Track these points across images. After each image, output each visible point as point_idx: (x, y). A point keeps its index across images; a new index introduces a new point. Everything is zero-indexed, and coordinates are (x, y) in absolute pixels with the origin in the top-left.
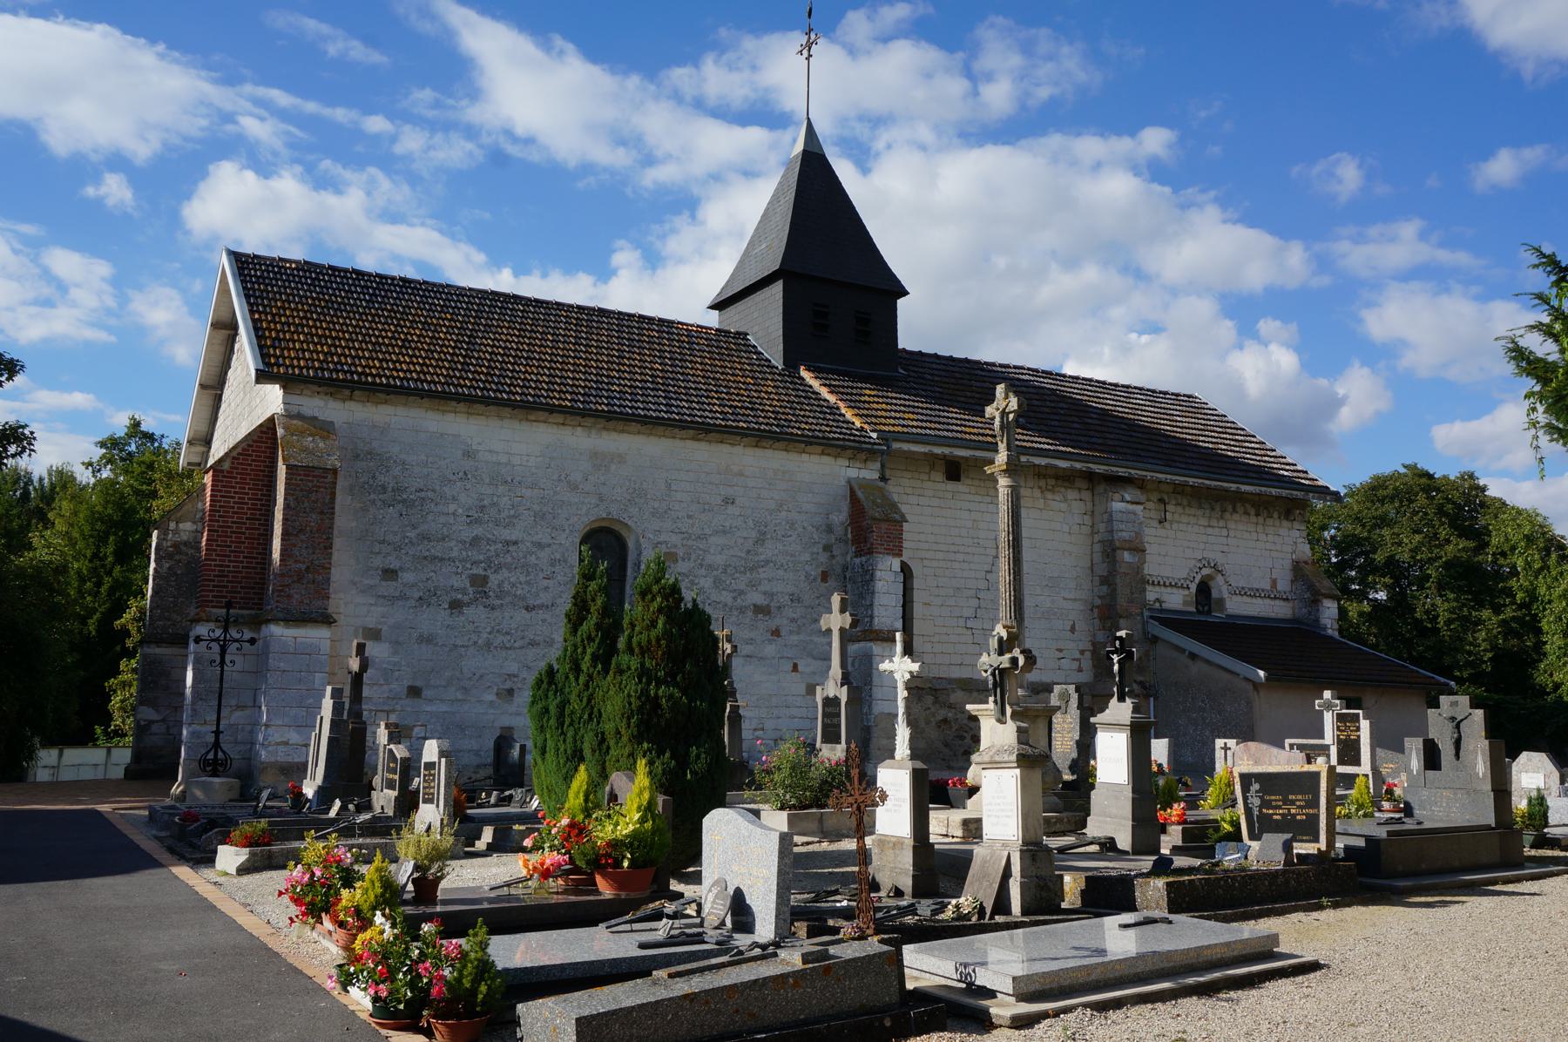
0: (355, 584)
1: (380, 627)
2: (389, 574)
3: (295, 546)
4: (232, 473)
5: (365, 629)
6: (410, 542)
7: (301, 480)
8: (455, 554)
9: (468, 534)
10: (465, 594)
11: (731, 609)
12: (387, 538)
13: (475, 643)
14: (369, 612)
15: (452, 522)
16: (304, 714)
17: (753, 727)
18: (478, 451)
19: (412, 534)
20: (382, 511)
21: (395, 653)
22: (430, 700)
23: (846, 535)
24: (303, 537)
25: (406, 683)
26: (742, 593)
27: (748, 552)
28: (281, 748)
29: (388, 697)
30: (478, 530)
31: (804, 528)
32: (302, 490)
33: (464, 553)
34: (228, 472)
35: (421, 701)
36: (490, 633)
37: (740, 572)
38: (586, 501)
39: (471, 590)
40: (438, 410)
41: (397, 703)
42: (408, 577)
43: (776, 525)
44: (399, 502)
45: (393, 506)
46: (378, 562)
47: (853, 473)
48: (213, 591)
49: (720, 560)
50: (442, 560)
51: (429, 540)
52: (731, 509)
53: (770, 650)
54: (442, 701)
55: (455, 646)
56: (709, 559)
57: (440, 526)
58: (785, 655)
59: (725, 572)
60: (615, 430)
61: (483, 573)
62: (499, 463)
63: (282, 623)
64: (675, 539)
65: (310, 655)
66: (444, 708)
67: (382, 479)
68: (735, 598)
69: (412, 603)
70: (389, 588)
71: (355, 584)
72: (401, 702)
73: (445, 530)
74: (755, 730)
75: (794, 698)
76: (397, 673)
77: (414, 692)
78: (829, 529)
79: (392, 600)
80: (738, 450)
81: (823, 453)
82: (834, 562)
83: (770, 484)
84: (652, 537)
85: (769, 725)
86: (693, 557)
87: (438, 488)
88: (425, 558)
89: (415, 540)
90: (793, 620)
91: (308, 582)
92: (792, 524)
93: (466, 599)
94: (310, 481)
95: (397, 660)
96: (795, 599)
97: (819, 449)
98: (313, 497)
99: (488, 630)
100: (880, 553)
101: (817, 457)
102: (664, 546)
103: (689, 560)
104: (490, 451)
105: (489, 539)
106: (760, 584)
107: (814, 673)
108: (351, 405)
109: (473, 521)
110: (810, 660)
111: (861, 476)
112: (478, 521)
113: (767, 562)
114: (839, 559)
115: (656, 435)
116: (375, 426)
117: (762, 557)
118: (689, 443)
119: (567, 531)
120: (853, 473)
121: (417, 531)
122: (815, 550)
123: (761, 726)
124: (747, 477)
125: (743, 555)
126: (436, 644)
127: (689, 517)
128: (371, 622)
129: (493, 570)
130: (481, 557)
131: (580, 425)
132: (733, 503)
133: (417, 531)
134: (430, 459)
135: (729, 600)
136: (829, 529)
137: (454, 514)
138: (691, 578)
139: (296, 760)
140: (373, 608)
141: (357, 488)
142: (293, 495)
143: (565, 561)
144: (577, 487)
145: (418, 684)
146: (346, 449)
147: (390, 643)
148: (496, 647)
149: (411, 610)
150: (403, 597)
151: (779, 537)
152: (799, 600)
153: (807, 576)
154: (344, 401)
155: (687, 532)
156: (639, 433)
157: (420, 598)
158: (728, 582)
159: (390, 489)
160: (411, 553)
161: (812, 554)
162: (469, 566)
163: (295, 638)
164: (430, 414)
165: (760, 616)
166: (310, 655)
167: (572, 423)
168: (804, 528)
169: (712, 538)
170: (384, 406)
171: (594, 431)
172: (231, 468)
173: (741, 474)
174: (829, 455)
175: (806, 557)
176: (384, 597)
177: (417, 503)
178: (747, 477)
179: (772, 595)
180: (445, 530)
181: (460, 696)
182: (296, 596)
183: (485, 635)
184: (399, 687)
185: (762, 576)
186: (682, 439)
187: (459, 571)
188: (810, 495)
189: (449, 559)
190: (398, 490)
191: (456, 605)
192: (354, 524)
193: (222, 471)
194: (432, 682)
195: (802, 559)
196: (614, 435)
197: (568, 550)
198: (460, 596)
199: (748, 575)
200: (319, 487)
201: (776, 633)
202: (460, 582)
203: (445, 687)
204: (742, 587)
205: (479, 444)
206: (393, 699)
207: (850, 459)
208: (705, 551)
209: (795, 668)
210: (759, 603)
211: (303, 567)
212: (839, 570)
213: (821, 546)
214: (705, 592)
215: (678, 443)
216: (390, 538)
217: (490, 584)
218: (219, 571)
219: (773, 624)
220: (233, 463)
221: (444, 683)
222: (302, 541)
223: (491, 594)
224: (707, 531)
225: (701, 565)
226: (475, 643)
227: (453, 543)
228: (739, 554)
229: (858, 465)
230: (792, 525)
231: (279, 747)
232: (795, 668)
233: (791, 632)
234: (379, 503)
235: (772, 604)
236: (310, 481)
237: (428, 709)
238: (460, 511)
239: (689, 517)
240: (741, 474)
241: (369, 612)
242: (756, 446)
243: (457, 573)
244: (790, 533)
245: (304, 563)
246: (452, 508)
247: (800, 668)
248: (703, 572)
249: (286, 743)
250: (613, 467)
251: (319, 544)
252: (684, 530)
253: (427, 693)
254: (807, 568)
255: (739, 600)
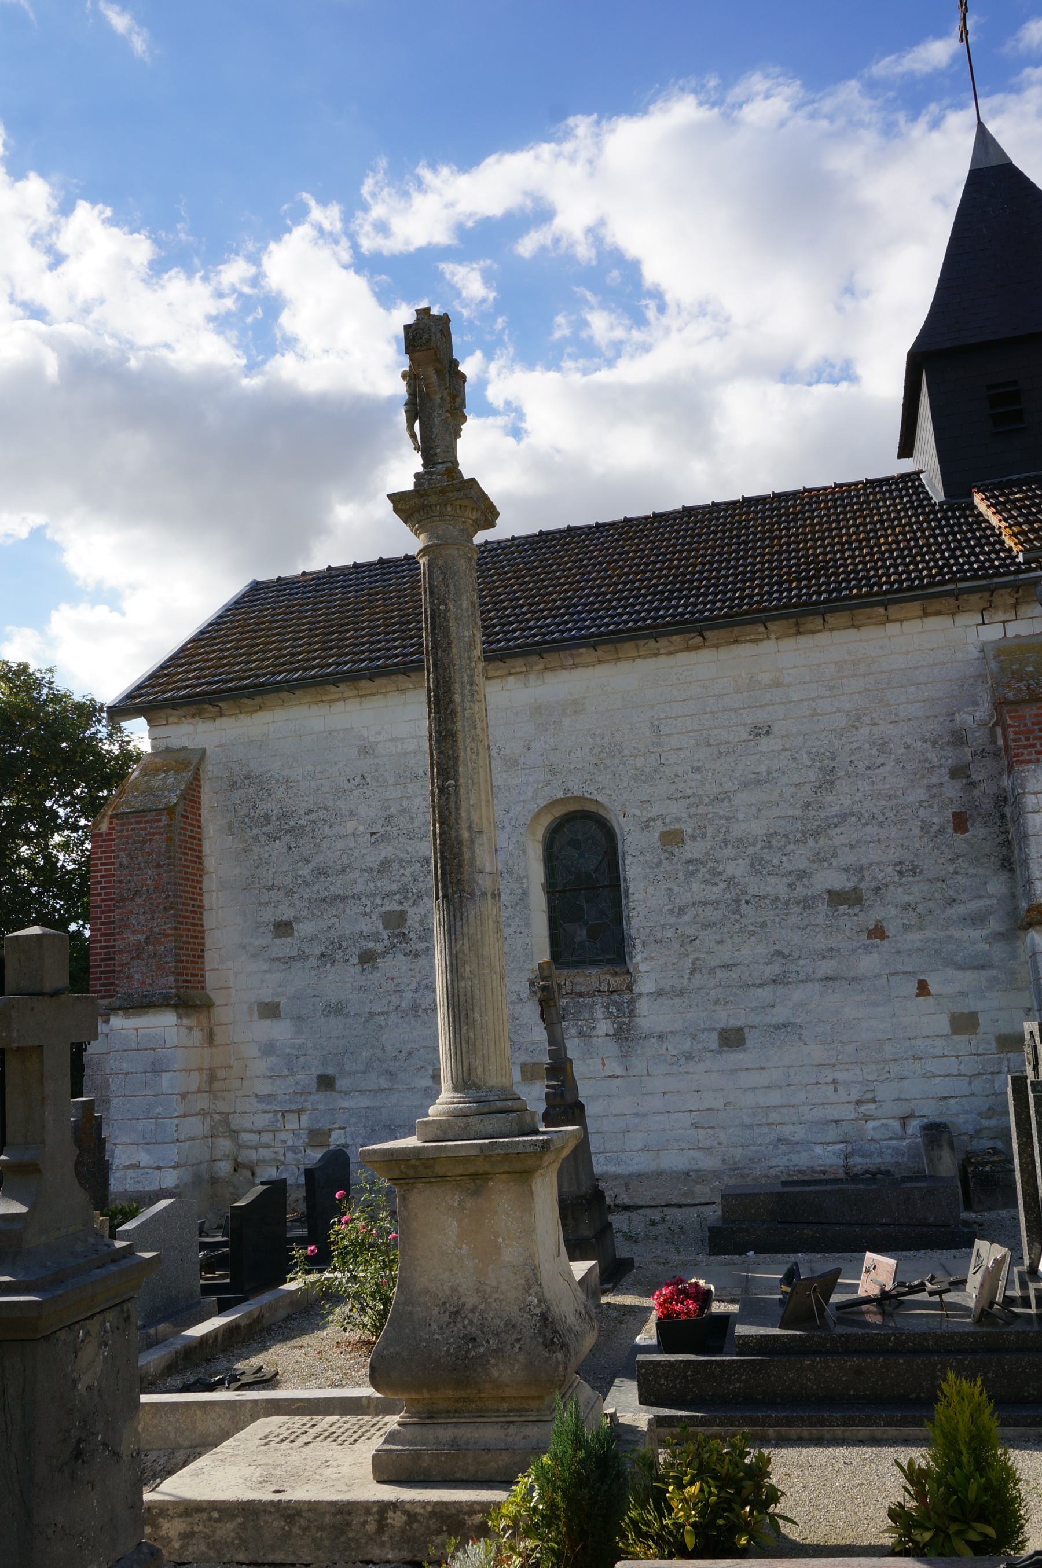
0: (244, 947)
1: (277, 1000)
2: (283, 928)
3: (131, 912)
4: (111, 834)
5: (260, 1004)
6: (304, 881)
7: (132, 830)
8: (359, 888)
9: (373, 859)
10: (378, 941)
11: (787, 904)
12: (276, 882)
13: (398, 1007)
14: (263, 981)
15: (352, 845)
16: (154, 1127)
17: (854, 1098)
18: (377, 743)
19: (305, 871)
20: (267, 848)
21: (299, 1032)
22: (346, 1093)
23: (994, 742)
24: (139, 900)
25: (315, 1072)
26: (802, 875)
27: (807, 805)
28: (130, 1173)
29: (295, 1093)
30: (387, 851)
31: (907, 747)
32: (135, 842)
33: (372, 885)
34: (107, 835)
35: (334, 1094)
36: (416, 991)
37: (797, 842)
38: (531, 779)
39: (385, 934)
40: (323, 701)
41: (306, 1101)
42: (305, 929)
43: (852, 752)
44: (287, 832)
45: (280, 838)
46: (269, 915)
47: (992, 633)
48: (100, 979)
49: (757, 828)
50: (344, 899)
51: (326, 875)
52: (765, 744)
53: (869, 963)
54: (361, 1092)
55: (372, 1014)
56: (738, 830)
57: (339, 853)
58: (900, 968)
59: (769, 845)
60: (563, 667)
61: (399, 908)
62: (406, 754)
63: (121, 1013)
64: (675, 809)
65: (154, 1049)
66: (364, 1102)
67: (264, 806)
68: (791, 886)
69: (314, 962)
70: (285, 946)
71: (244, 947)
72: (311, 1098)
73: (345, 857)
74: (859, 1103)
75: (929, 1042)
76: (302, 1059)
77: (326, 1082)
78: (959, 738)
79: (287, 961)
80: (768, 646)
81: (926, 614)
82: (976, 793)
83: (831, 688)
84: (637, 812)
85: (885, 1092)
86: (710, 830)
87: (330, 804)
88: (324, 900)
89: (309, 878)
90: (907, 907)
91: (149, 956)
92: (883, 744)
93: (380, 947)
94: (142, 829)
95: (300, 1041)
96: (907, 870)
97: (915, 607)
98: (147, 848)
99: (413, 987)
100: (1029, 762)
101: (918, 621)
102: (659, 823)
103: (704, 836)
104: (392, 740)
105: (402, 860)
106: (835, 855)
107: (962, 994)
108: (224, 722)
109: (378, 838)
110: (950, 972)
111: (1010, 634)
112: (385, 838)
113: (844, 817)
114: (988, 788)
115: (627, 659)
116: (252, 741)
117: (835, 810)
118: (683, 657)
119: (508, 829)
120: (992, 633)
121: (311, 866)
122: (934, 780)
123: (869, 1096)
124: (789, 685)
125: (798, 813)
126: (347, 1016)
127: (696, 770)
128: (267, 995)
129: (411, 902)
130: (395, 887)
131: (510, 674)
132: (768, 733)
133: (311, 866)
134: (319, 768)
135: (782, 891)
136: (959, 738)
137: (354, 834)
138: (710, 864)
139: (147, 1189)
140: (268, 976)
141: (236, 824)
142: (124, 850)
143: (510, 872)
144: (516, 763)
145: (330, 1071)
146: (221, 778)
147: (291, 1019)
148: (426, 1010)
149: (313, 973)
150: (302, 957)
151: (861, 770)
152: (914, 871)
153: (925, 827)
154: (214, 719)
155: (694, 795)
156: (600, 662)
157: (323, 955)
158: (775, 861)
159: (274, 818)
160: (306, 896)
161: (929, 787)
162: (379, 901)
163: (137, 1030)
164: (315, 710)
165: (843, 909)
166: (154, 1049)
167: (498, 673)
168: (907, 747)
169: (739, 795)
170: (260, 713)
171: (532, 677)
172: (110, 829)
173: (777, 684)
174: (938, 613)
175: (920, 794)
176: (278, 959)
177: (307, 829)
178: (789, 685)
179: (861, 870)
180: (345, 857)
181: (384, 1084)
182: (136, 976)
183: (408, 995)
184: (307, 1078)
185: (837, 842)
186: (670, 653)
187: (368, 910)
188: (913, 688)
189: (353, 897)
190: (284, 816)
191: (367, 958)
192: (237, 871)
193: (101, 835)
194: (347, 1068)
195: (911, 799)
196: (564, 675)
197: (511, 855)
198: (371, 945)
199: (811, 842)
200: (153, 834)
201: (878, 932)
202: (372, 924)
203: (364, 1073)
204: (803, 864)
205: (379, 733)
206: (302, 1094)
207: (953, 614)
208: (729, 819)
209: (923, 988)
210: (837, 886)
211: (142, 937)
212: (987, 805)
213: (944, 771)
214: (736, 884)
215: (663, 661)
216: (279, 881)
217: (409, 923)
218: (105, 953)
219: (869, 919)
220: (111, 823)
221: (362, 1068)
222: (139, 905)
223: (412, 935)
224: (729, 786)
225: (725, 842)
226: (398, 1007)
227: (356, 875)
228: (790, 813)
229: (1001, 616)
230: (883, 746)
231: (128, 1171)
232: (923, 988)
233: (906, 928)
234: (263, 838)
235: (863, 885)
236: (142, 829)
237: (346, 1104)
238: (361, 828)
239: (696, 770)
240: (777, 684)
241: (263, 981)
242: (799, 633)
243: (365, 914)
244: (879, 762)
245: (142, 932)
246: (350, 826)
247: (933, 987)
248: (729, 851)
249: (136, 1166)
250: (566, 721)
251: (158, 905)
252: (689, 792)
253: (342, 1083)
254: (922, 812)
255: (799, 889)
